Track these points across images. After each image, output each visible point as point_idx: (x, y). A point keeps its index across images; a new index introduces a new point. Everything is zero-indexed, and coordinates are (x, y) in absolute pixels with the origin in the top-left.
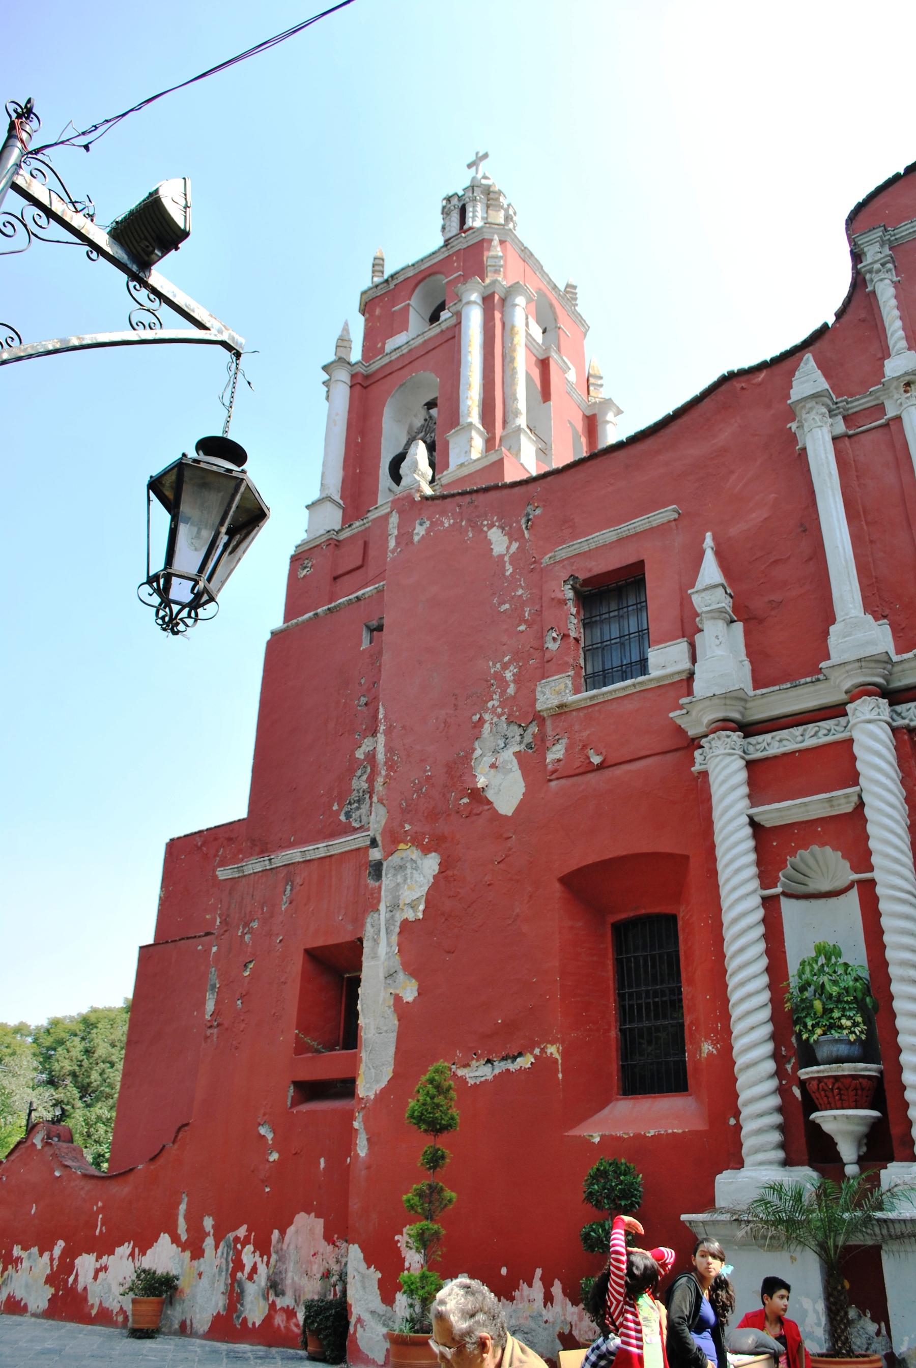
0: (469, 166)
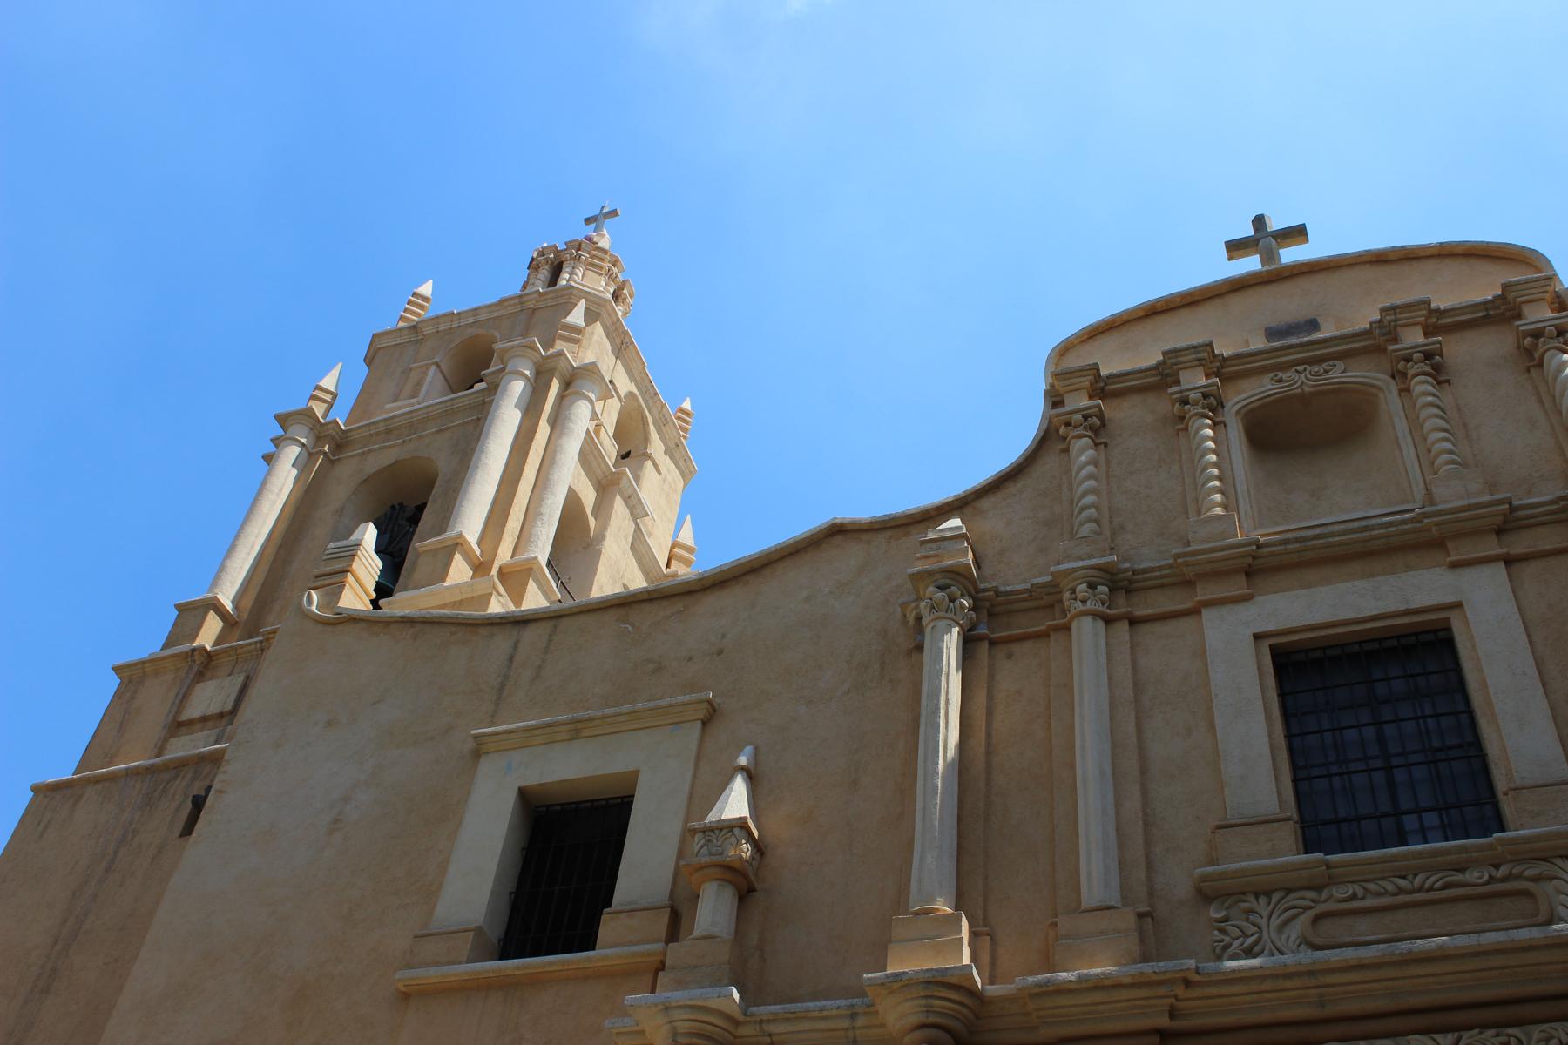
0: (588, 221)
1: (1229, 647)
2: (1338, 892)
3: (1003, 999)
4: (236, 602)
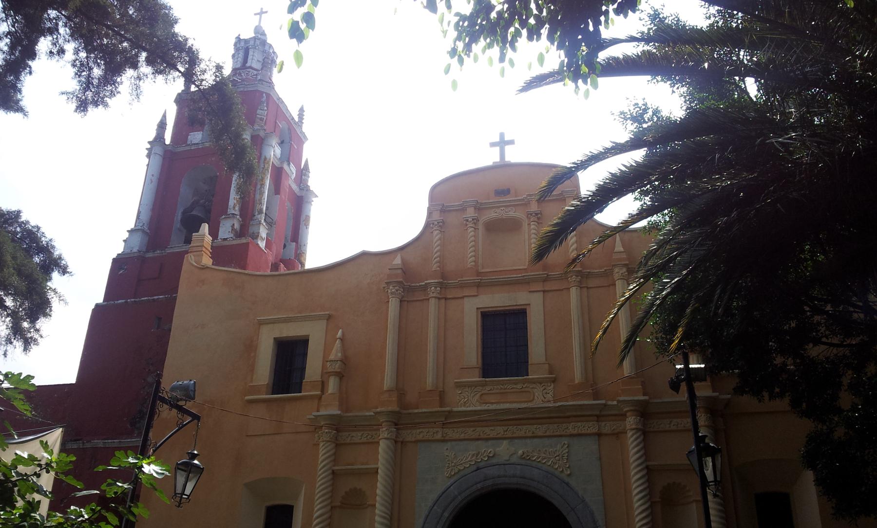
1: (469, 311)
2: (488, 388)
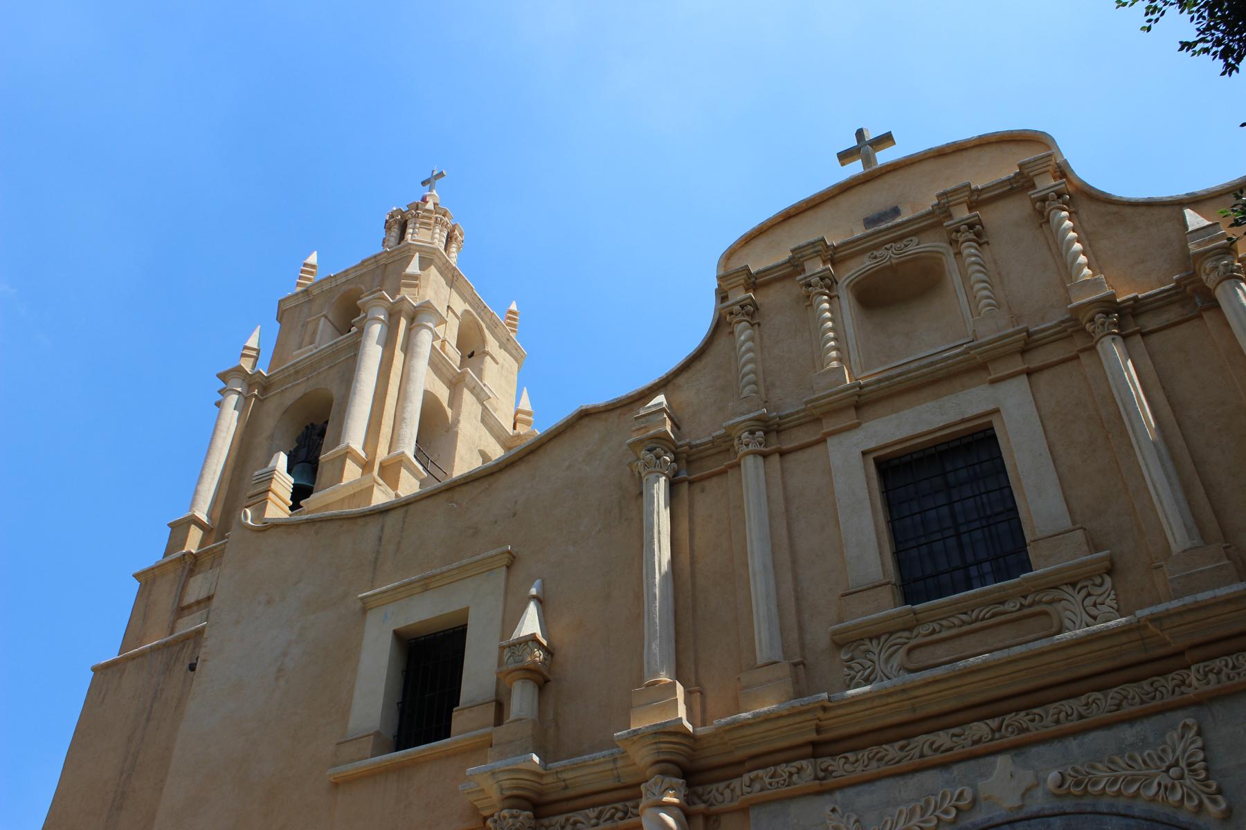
0: (424, 183)
2: (924, 630)
3: (707, 736)
4: (210, 515)
